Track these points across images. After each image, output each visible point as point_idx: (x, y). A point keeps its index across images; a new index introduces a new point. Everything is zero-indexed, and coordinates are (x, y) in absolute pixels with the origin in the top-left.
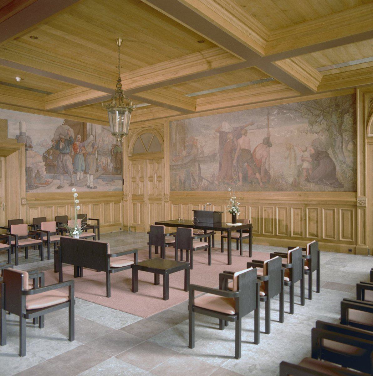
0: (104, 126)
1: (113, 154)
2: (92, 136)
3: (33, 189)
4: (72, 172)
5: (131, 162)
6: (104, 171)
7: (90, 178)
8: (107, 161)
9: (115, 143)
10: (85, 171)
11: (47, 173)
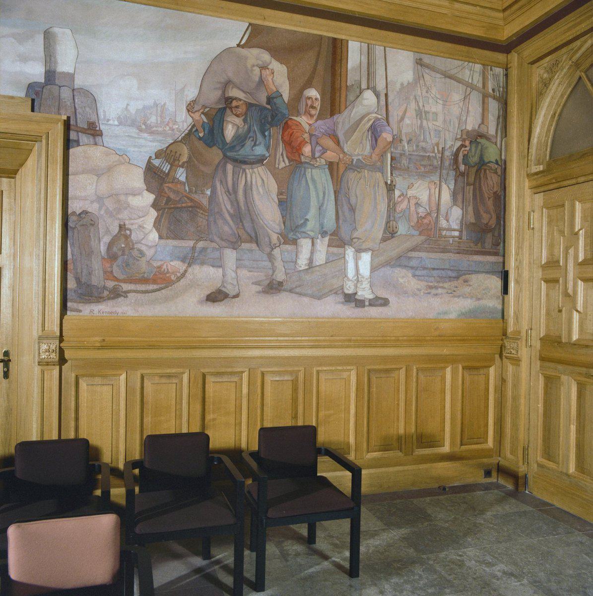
0: (423, 56)
1: (462, 168)
2: (369, 96)
3: (99, 299)
4: (274, 238)
5: (539, 199)
6: (423, 238)
7: (360, 263)
8: (434, 198)
9: (471, 124)
10: (335, 233)
11: (161, 237)
